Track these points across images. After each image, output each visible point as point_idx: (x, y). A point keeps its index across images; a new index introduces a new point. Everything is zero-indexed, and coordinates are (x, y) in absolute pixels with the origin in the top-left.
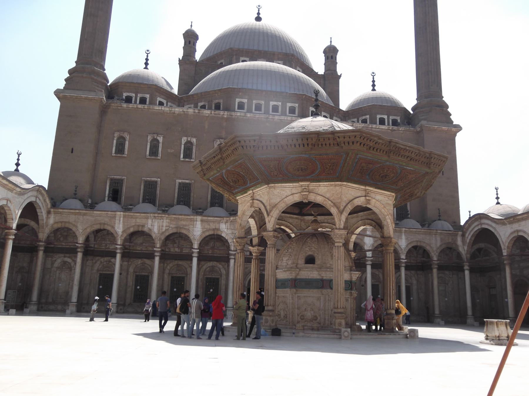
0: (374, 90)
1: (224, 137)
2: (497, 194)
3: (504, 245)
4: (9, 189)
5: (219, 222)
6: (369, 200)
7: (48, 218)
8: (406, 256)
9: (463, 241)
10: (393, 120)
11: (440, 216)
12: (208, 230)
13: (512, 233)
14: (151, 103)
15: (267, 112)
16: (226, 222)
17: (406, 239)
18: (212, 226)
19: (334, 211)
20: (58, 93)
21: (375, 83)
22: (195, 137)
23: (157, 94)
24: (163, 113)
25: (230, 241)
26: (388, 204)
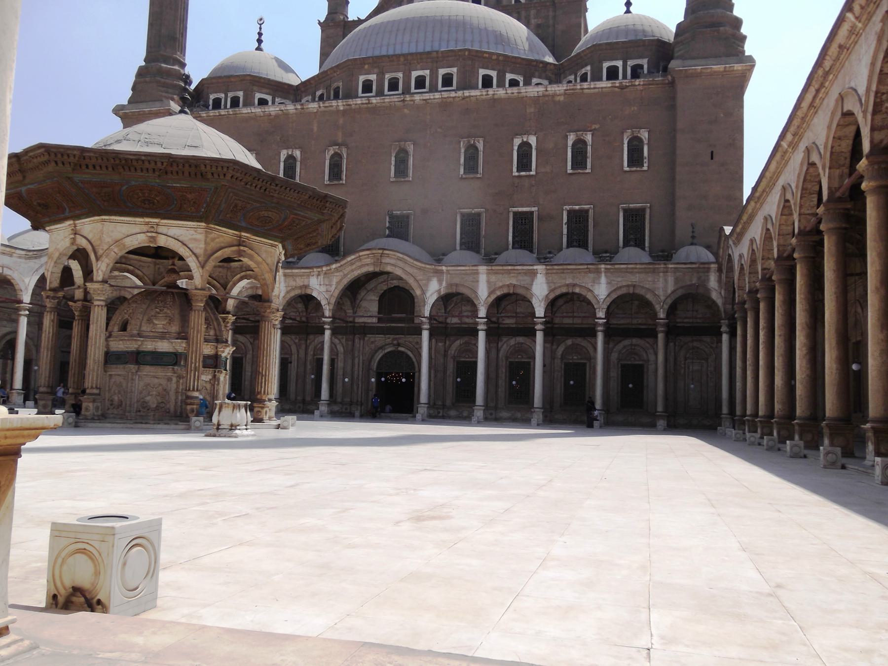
0: (628, 11)
1: (340, 141)
5: (309, 276)
6: (151, 237)
11: (693, 237)
12: (293, 289)
15: (406, 91)
16: (318, 275)
17: (608, 283)
18: (300, 282)
19: (92, 257)
22: (296, 148)
23: (255, 88)
24: (255, 118)
25: (323, 303)
26: (195, 240)
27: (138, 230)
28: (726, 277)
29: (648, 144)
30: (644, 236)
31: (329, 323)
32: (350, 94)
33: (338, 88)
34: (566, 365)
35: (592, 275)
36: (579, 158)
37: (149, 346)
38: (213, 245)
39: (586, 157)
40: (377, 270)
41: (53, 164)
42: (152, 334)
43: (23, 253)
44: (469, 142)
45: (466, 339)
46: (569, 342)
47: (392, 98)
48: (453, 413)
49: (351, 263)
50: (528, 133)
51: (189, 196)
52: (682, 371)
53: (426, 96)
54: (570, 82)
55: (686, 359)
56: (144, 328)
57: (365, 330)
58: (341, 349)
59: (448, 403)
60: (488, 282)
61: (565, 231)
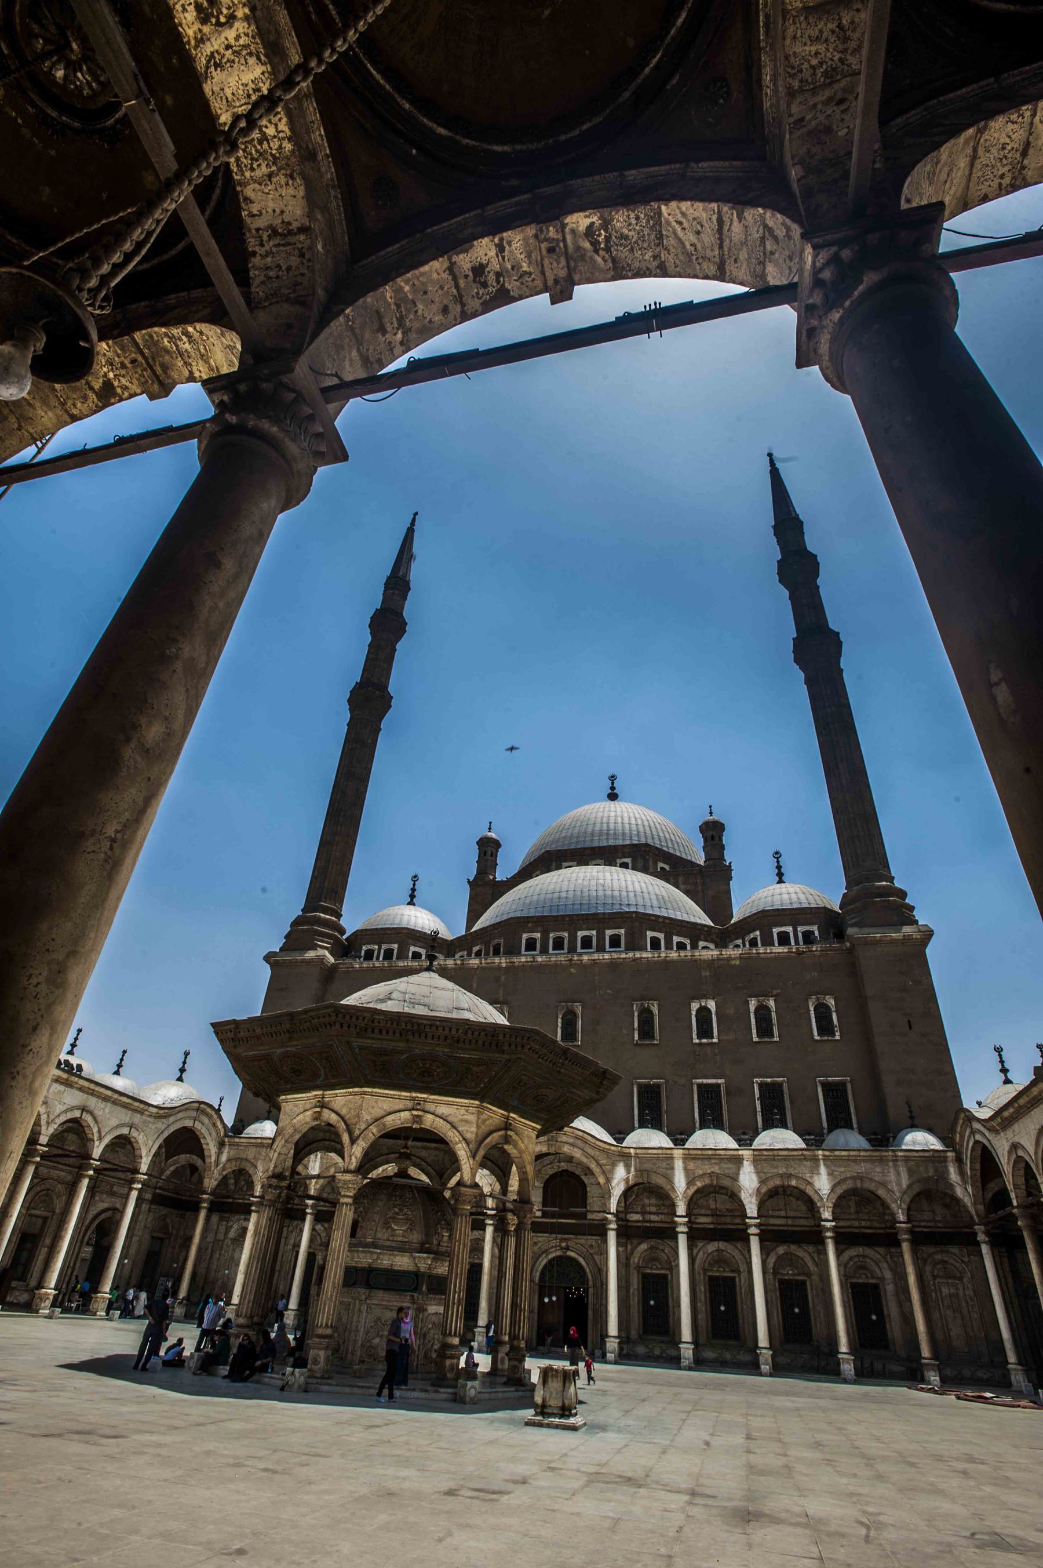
1: (501, 999)
2: (1002, 1062)
4: (135, 1111)
6: (418, 1116)
7: (219, 1153)
8: (833, 1213)
9: (961, 1173)
10: (804, 933)
11: (912, 1118)
14: (398, 958)
15: (572, 950)
17: (830, 1174)
19: (345, 1138)
20: (268, 958)
21: (783, 870)
23: (410, 941)
26: (467, 1121)
27: (401, 1107)
28: (971, 1169)
29: (836, 1011)
30: (850, 1114)
31: (492, 1217)
32: (513, 950)
33: (499, 944)
34: (781, 1282)
35: (808, 1164)
36: (764, 1025)
37: (386, 1261)
38: (484, 1129)
39: (771, 1025)
41: (338, 1026)
42: (388, 1243)
43: (155, 1110)
44: (642, 1004)
45: (653, 1242)
46: (781, 1250)
47: (558, 957)
48: (641, 1350)
51: (474, 1069)
52: (934, 1295)
53: (596, 956)
54: (737, 946)
55: (934, 1277)
56: (379, 1235)
59: (634, 1334)
60: (686, 1170)
61: (759, 1108)
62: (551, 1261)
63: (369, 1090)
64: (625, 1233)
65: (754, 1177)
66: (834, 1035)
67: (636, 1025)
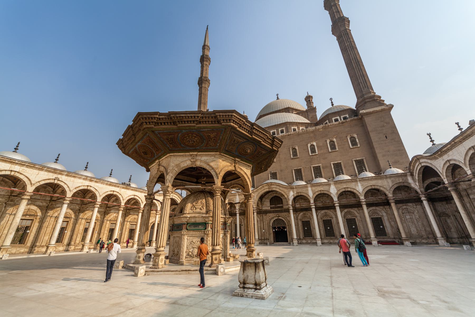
3: (443, 175)
9: (413, 179)
13: (444, 164)
17: (362, 185)
28: (418, 177)
34: (347, 219)
39: (335, 146)
40: (270, 190)
41: (145, 124)
45: (304, 212)
46: (346, 210)
48: (304, 241)
49: (261, 188)
50: (312, 141)
57: (266, 212)
58: (259, 219)
59: (301, 237)
60: (312, 190)
61: (334, 171)
62: (274, 221)
63: (172, 154)
64: (295, 210)
65: (335, 189)
66: (357, 145)
67: (291, 153)
